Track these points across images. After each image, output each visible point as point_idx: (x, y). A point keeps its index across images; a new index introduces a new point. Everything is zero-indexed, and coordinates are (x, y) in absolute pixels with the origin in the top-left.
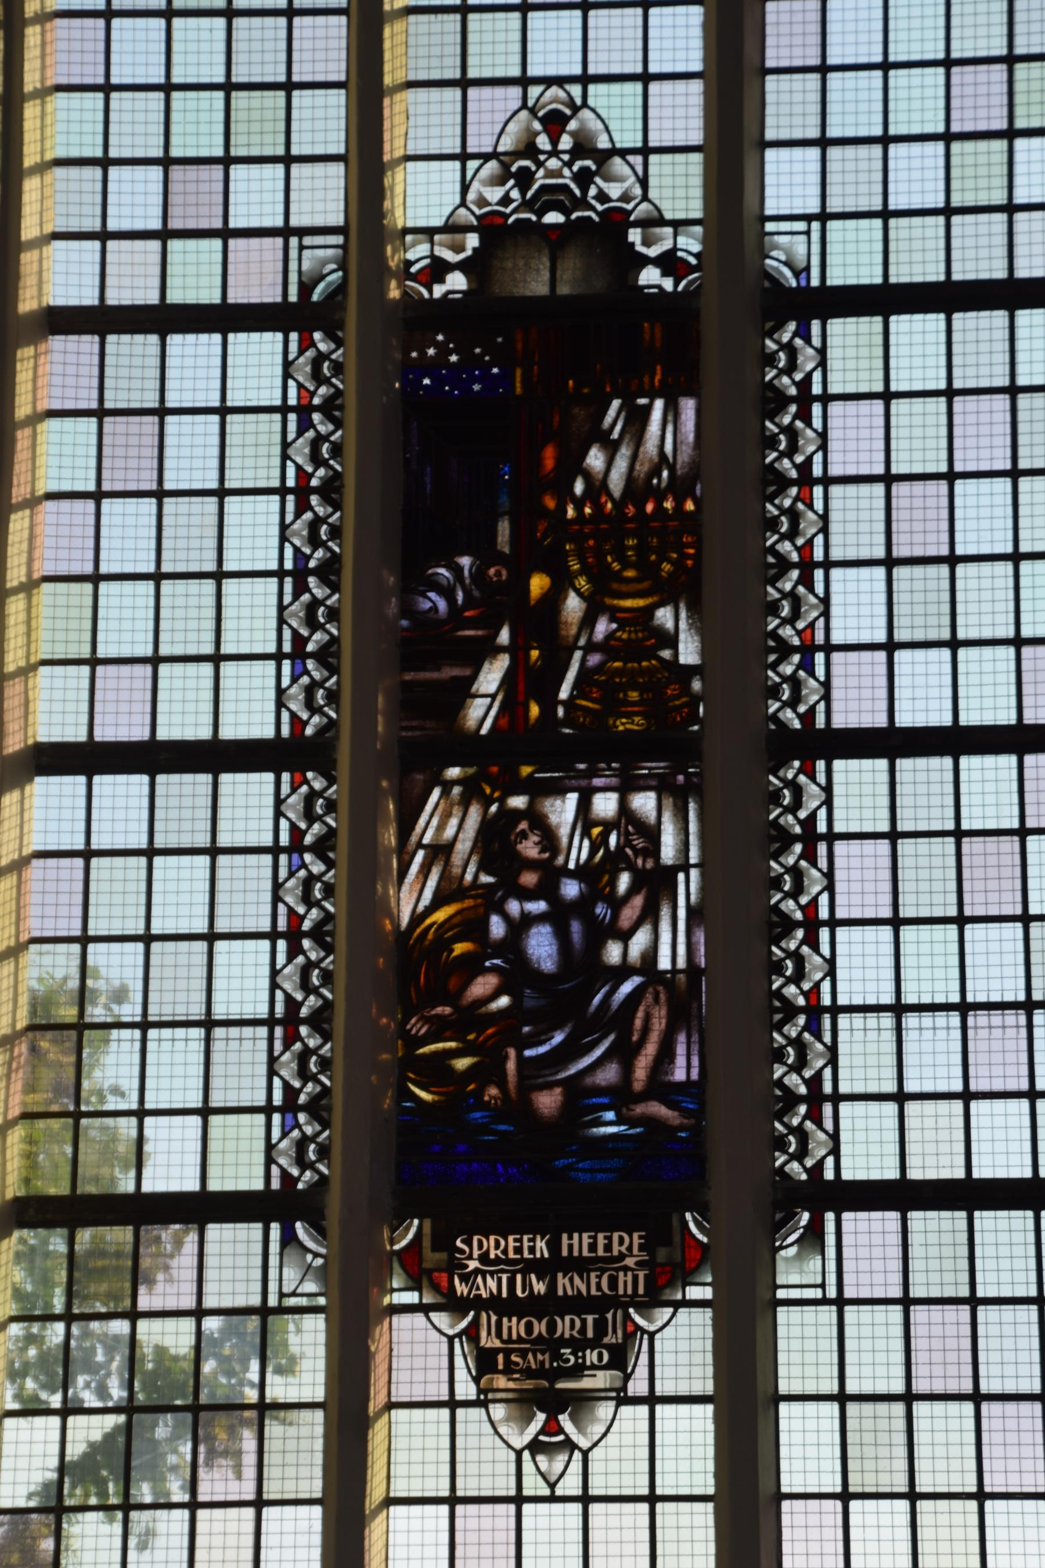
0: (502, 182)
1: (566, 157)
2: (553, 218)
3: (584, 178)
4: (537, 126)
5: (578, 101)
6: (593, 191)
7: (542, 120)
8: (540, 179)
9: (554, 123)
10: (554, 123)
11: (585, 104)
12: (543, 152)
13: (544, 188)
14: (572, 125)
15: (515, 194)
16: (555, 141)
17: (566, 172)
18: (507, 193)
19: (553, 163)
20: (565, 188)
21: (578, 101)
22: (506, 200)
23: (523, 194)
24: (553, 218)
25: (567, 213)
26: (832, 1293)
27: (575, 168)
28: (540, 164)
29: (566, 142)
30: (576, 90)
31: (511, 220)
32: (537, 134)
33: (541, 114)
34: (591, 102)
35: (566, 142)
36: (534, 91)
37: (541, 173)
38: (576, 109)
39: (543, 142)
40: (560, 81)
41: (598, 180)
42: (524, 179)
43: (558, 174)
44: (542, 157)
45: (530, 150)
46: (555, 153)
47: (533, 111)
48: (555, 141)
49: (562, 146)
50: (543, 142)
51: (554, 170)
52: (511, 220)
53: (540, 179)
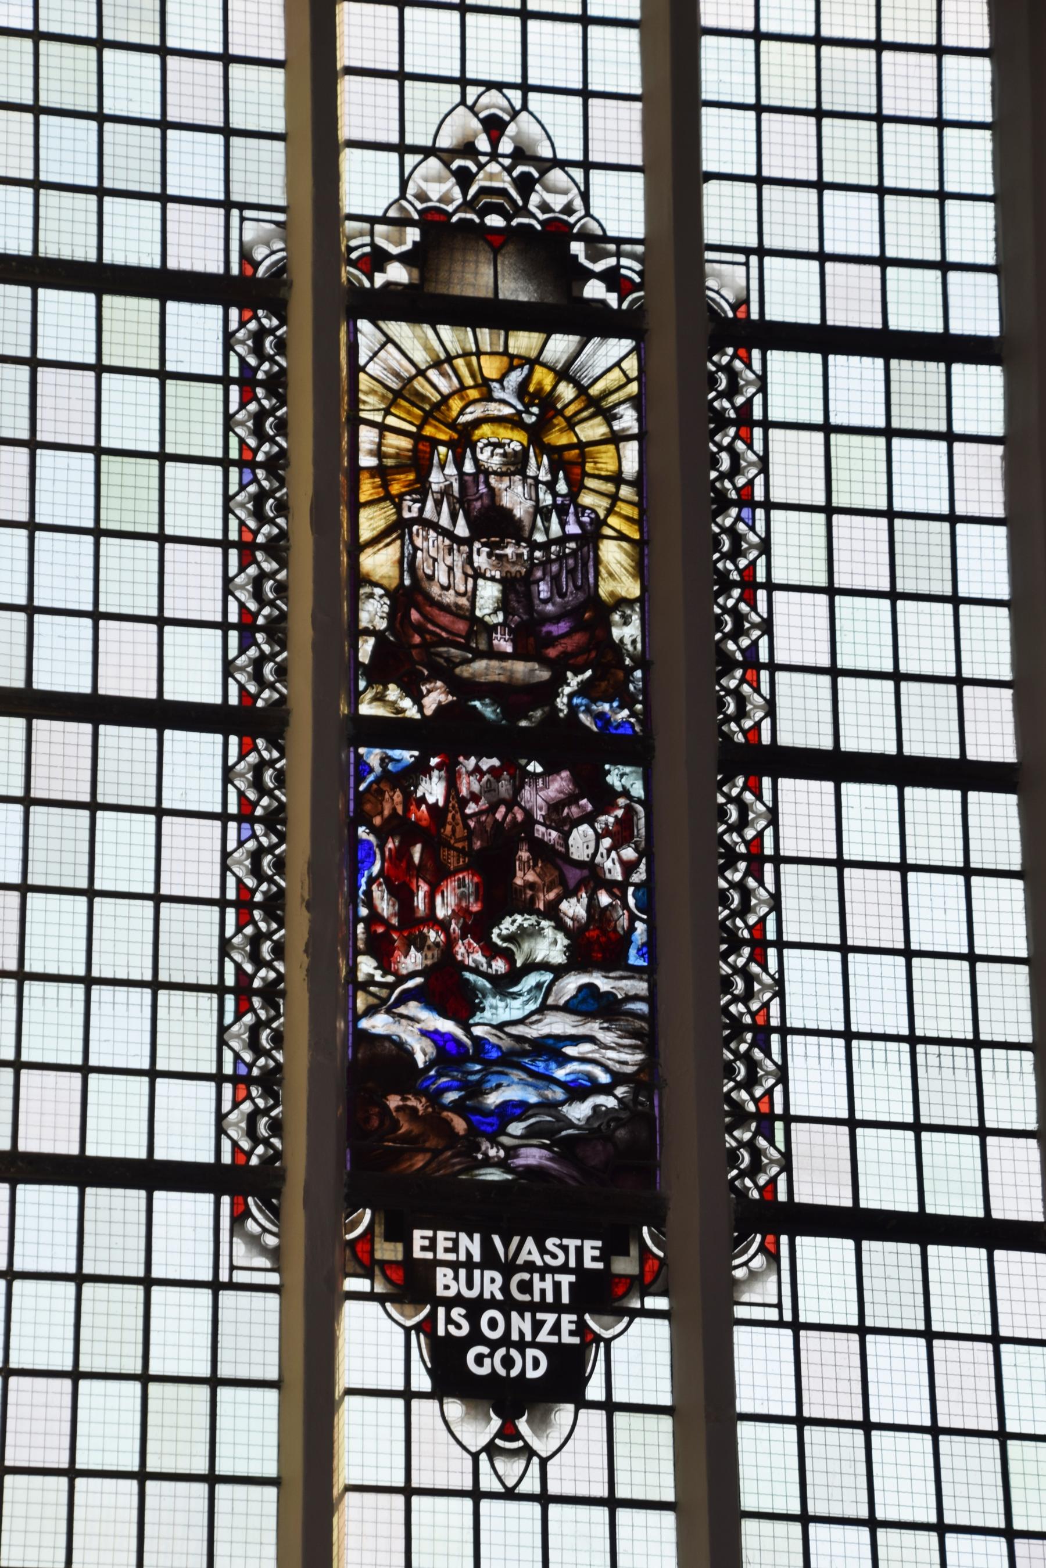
1: (507, 162)
2: (495, 221)
3: (525, 185)
5: (518, 106)
6: (534, 199)
7: (483, 121)
8: (481, 181)
9: (494, 127)
10: (494, 127)
11: (525, 107)
12: (484, 154)
13: (483, 191)
14: (511, 130)
15: (457, 193)
16: (494, 143)
18: (449, 191)
19: (494, 168)
20: (503, 192)
21: (518, 106)
22: (446, 199)
23: (465, 193)
24: (495, 221)
25: (508, 218)
26: (788, 1317)
27: (515, 174)
28: (481, 167)
29: (506, 146)
30: (516, 96)
33: (482, 115)
34: (531, 106)
35: (506, 146)
36: (472, 92)
37: (481, 175)
38: (514, 114)
39: (483, 144)
40: (500, 86)
42: (464, 178)
44: (483, 159)
45: (468, 149)
46: (494, 156)
48: (494, 143)
49: (500, 151)
50: (483, 144)
51: (495, 176)
53: (481, 181)
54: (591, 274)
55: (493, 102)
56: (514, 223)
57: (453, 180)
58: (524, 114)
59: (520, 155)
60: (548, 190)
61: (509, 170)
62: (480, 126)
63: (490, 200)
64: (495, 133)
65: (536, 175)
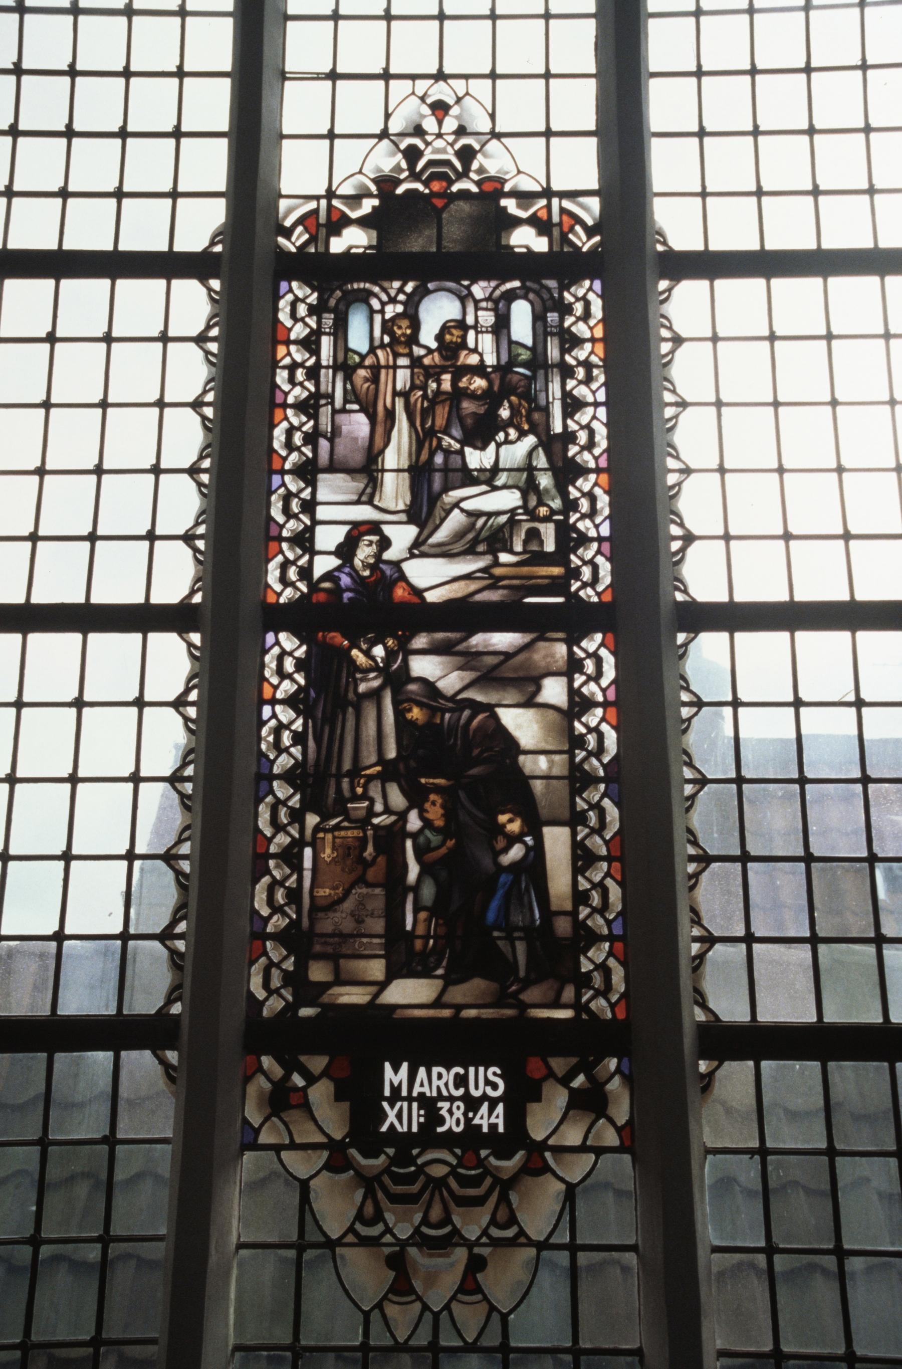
0: (394, 155)
1: (451, 138)
3: (467, 155)
4: (426, 110)
6: (475, 166)
10: (440, 109)
13: (431, 163)
14: (455, 111)
16: (440, 123)
17: (449, 149)
18: (398, 164)
19: (439, 144)
20: (448, 163)
27: (457, 146)
28: (428, 144)
29: (450, 124)
31: (400, 191)
32: (424, 116)
35: (450, 124)
37: (430, 149)
39: (430, 125)
41: (479, 156)
42: (412, 154)
43: (443, 151)
44: (429, 138)
45: (419, 131)
46: (439, 135)
47: (423, 99)
48: (440, 123)
50: (430, 125)
51: (440, 149)
52: (400, 191)
54: (517, 222)
55: (441, 92)
56: (455, 188)
57: (400, 156)
58: (468, 97)
59: (461, 131)
60: (485, 156)
61: (452, 145)
62: (429, 112)
63: (440, 172)
64: (440, 113)
65: (477, 147)
